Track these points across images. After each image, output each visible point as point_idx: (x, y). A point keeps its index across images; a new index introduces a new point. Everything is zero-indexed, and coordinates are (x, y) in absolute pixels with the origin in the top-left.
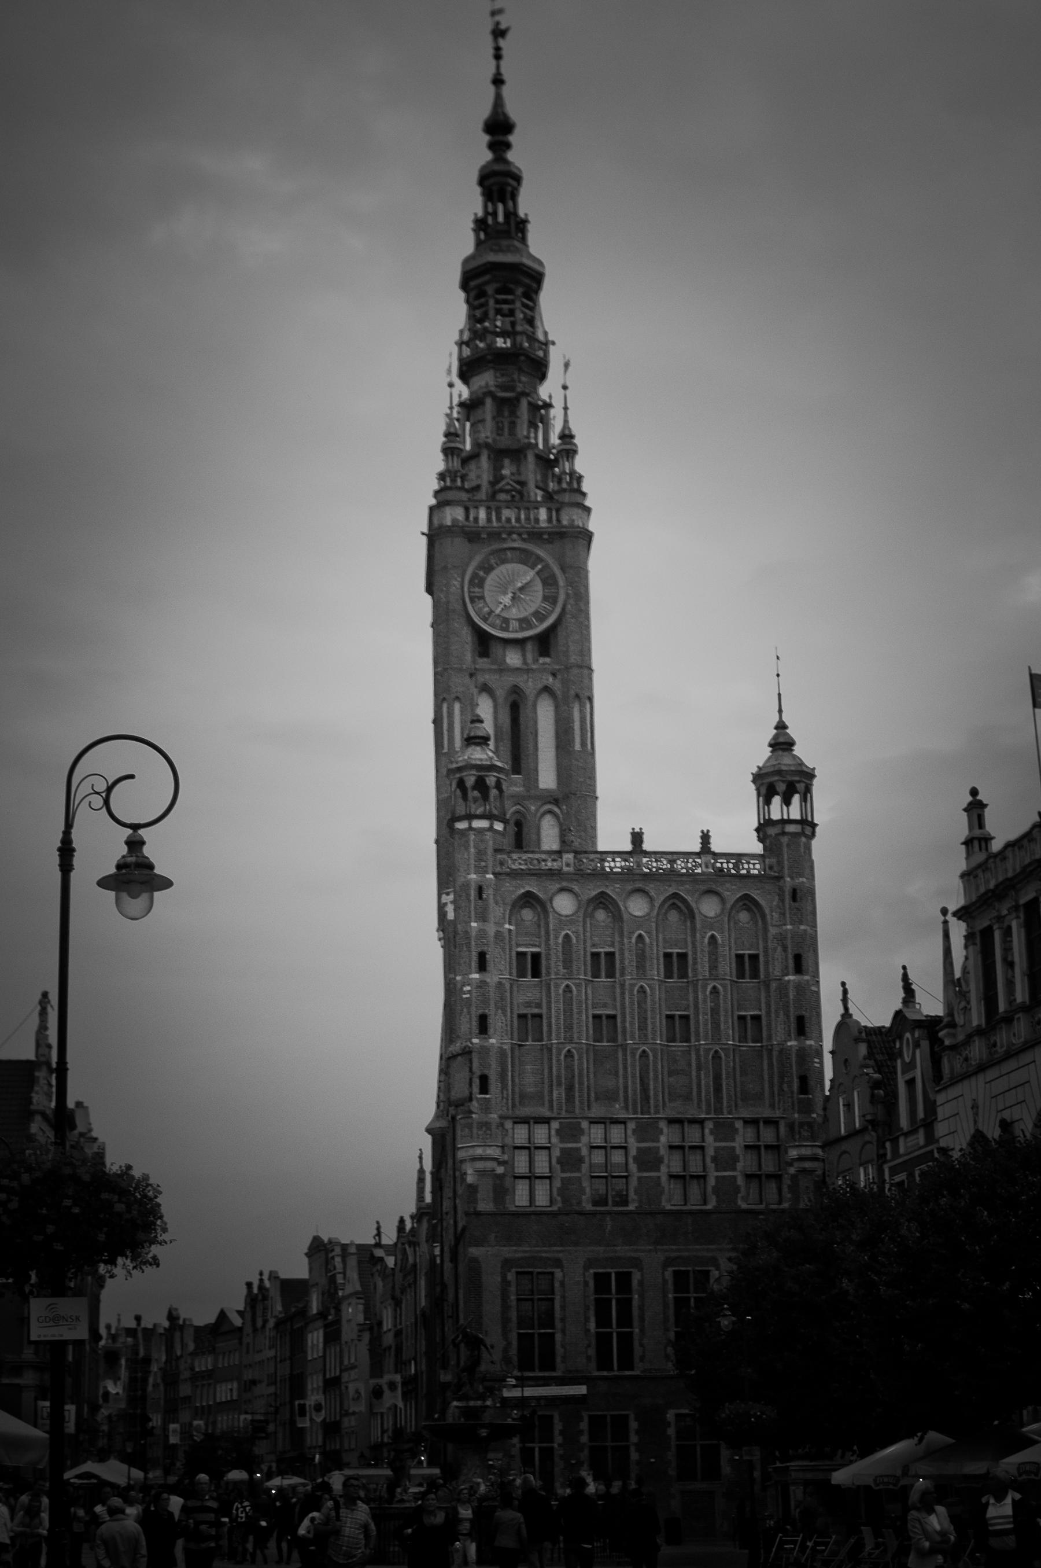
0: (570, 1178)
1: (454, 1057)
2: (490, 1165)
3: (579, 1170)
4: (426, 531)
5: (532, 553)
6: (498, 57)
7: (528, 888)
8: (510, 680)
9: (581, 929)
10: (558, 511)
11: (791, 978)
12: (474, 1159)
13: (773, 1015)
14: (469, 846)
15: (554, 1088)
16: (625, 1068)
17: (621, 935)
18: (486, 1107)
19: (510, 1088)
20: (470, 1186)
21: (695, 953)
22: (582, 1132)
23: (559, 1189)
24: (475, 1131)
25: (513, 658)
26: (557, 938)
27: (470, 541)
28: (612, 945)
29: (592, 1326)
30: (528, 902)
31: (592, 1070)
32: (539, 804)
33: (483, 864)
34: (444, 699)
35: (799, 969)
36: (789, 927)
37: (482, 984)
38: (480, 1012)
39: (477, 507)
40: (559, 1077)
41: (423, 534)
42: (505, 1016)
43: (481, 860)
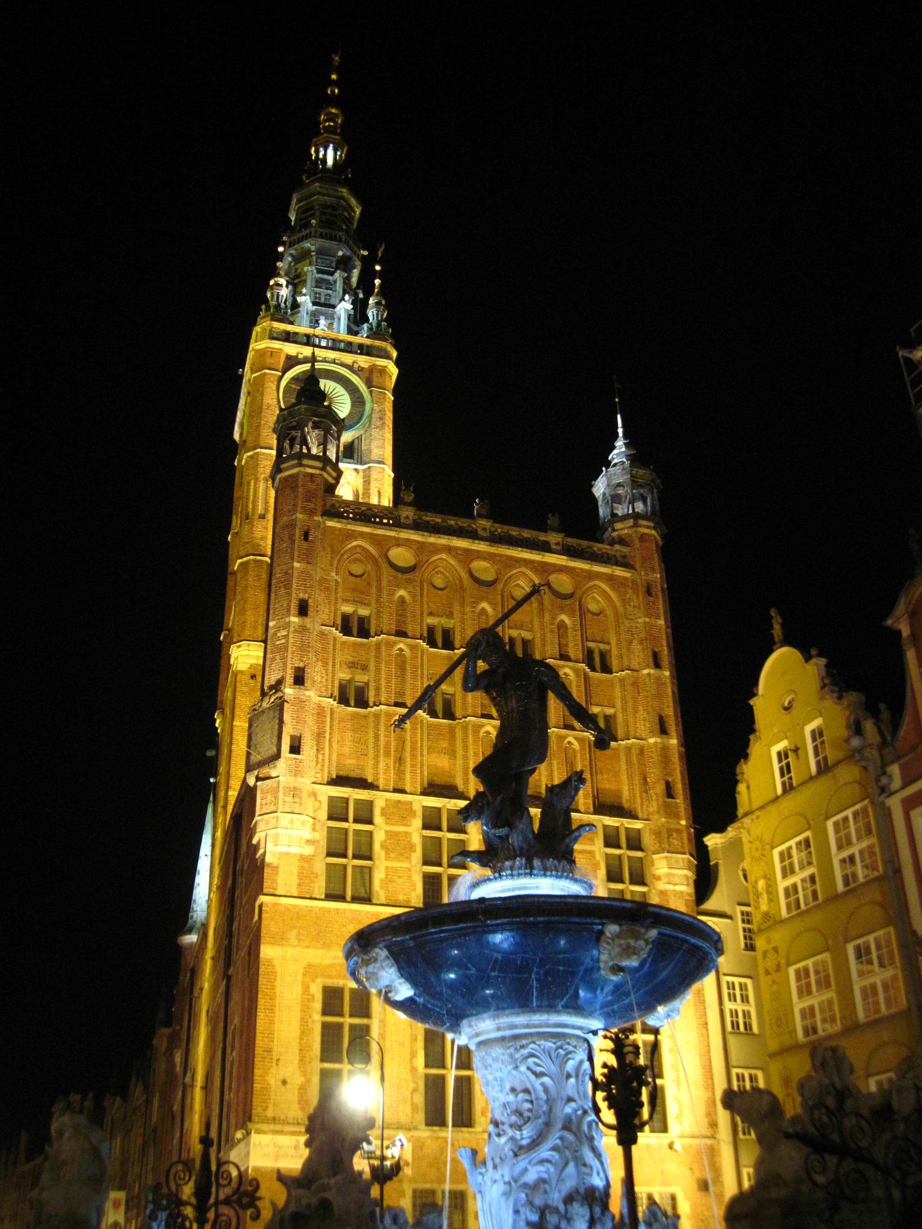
0: (396, 870)
3: (409, 858)
9: (418, 588)
11: (652, 671)
13: (630, 710)
14: (297, 485)
15: (381, 758)
16: (466, 748)
17: (463, 604)
18: (296, 772)
19: (327, 753)
21: (543, 635)
22: (415, 812)
23: (381, 881)
24: (281, 796)
26: (391, 594)
28: (450, 616)
29: (420, 1061)
31: (425, 744)
33: (312, 506)
35: (657, 665)
36: (647, 620)
37: (303, 629)
40: (388, 744)
42: (327, 670)
43: (309, 501)
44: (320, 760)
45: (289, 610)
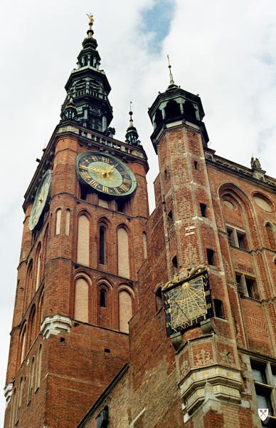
1: (176, 286)
2: (235, 394)
4: (40, 159)
5: (117, 163)
6: (91, 24)
7: (231, 181)
8: (101, 213)
10: (131, 151)
12: (216, 381)
20: (212, 412)
25: (103, 204)
27: (81, 146)
30: (229, 195)
32: (120, 282)
34: (59, 209)
38: (208, 247)
39: (86, 133)
41: (38, 160)
44: (239, 329)
45: (192, 212)
